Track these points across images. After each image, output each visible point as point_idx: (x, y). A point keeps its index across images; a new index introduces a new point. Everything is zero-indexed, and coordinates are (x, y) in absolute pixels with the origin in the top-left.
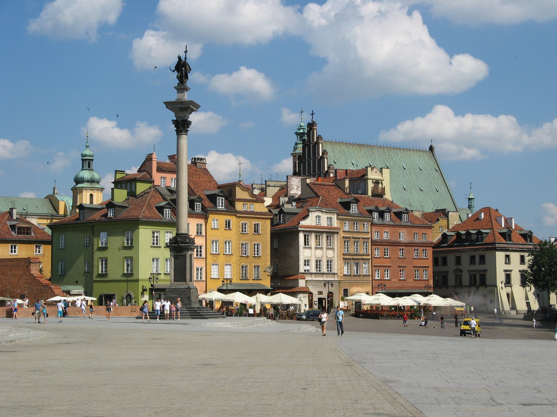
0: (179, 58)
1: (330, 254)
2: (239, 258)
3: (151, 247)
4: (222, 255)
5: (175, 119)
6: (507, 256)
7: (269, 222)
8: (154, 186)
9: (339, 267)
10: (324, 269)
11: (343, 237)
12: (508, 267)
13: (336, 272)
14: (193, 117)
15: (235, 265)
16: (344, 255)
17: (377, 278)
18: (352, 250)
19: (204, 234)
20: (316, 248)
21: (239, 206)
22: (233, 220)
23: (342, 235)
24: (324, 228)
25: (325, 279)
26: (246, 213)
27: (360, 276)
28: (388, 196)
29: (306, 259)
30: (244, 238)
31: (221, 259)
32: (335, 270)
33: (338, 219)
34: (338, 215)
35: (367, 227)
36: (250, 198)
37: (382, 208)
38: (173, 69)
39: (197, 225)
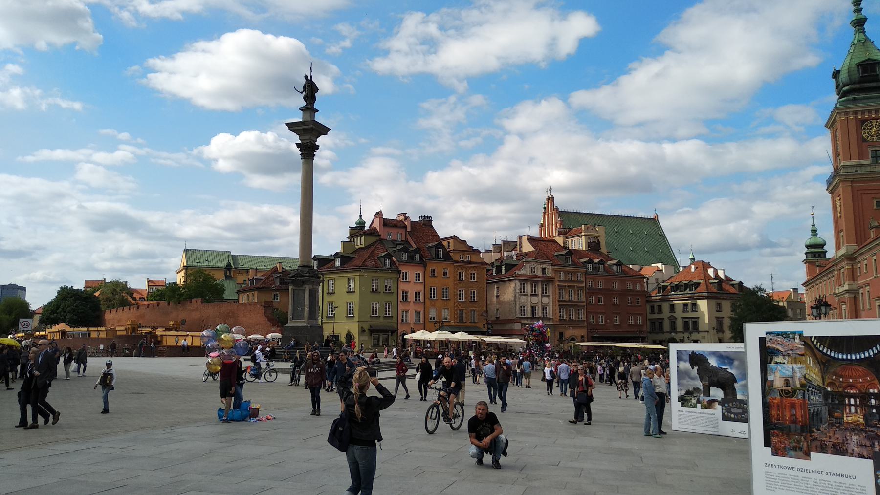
0: (306, 77)
1: (545, 300)
5: (300, 142)
6: (719, 305)
7: (485, 271)
8: (381, 240)
10: (539, 314)
12: (719, 314)
14: (321, 141)
16: (559, 301)
18: (566, 297)
20: (532, 295)
21: (456, 257)
22: (449, 268)
23: (557, 284)
24: (539, 277)
26: (463, 262)
28: (604, 250)
32: (550, 314)
34: (552, 265)
35: (581, 278)
37: (596, 261)
38: (302, 90)
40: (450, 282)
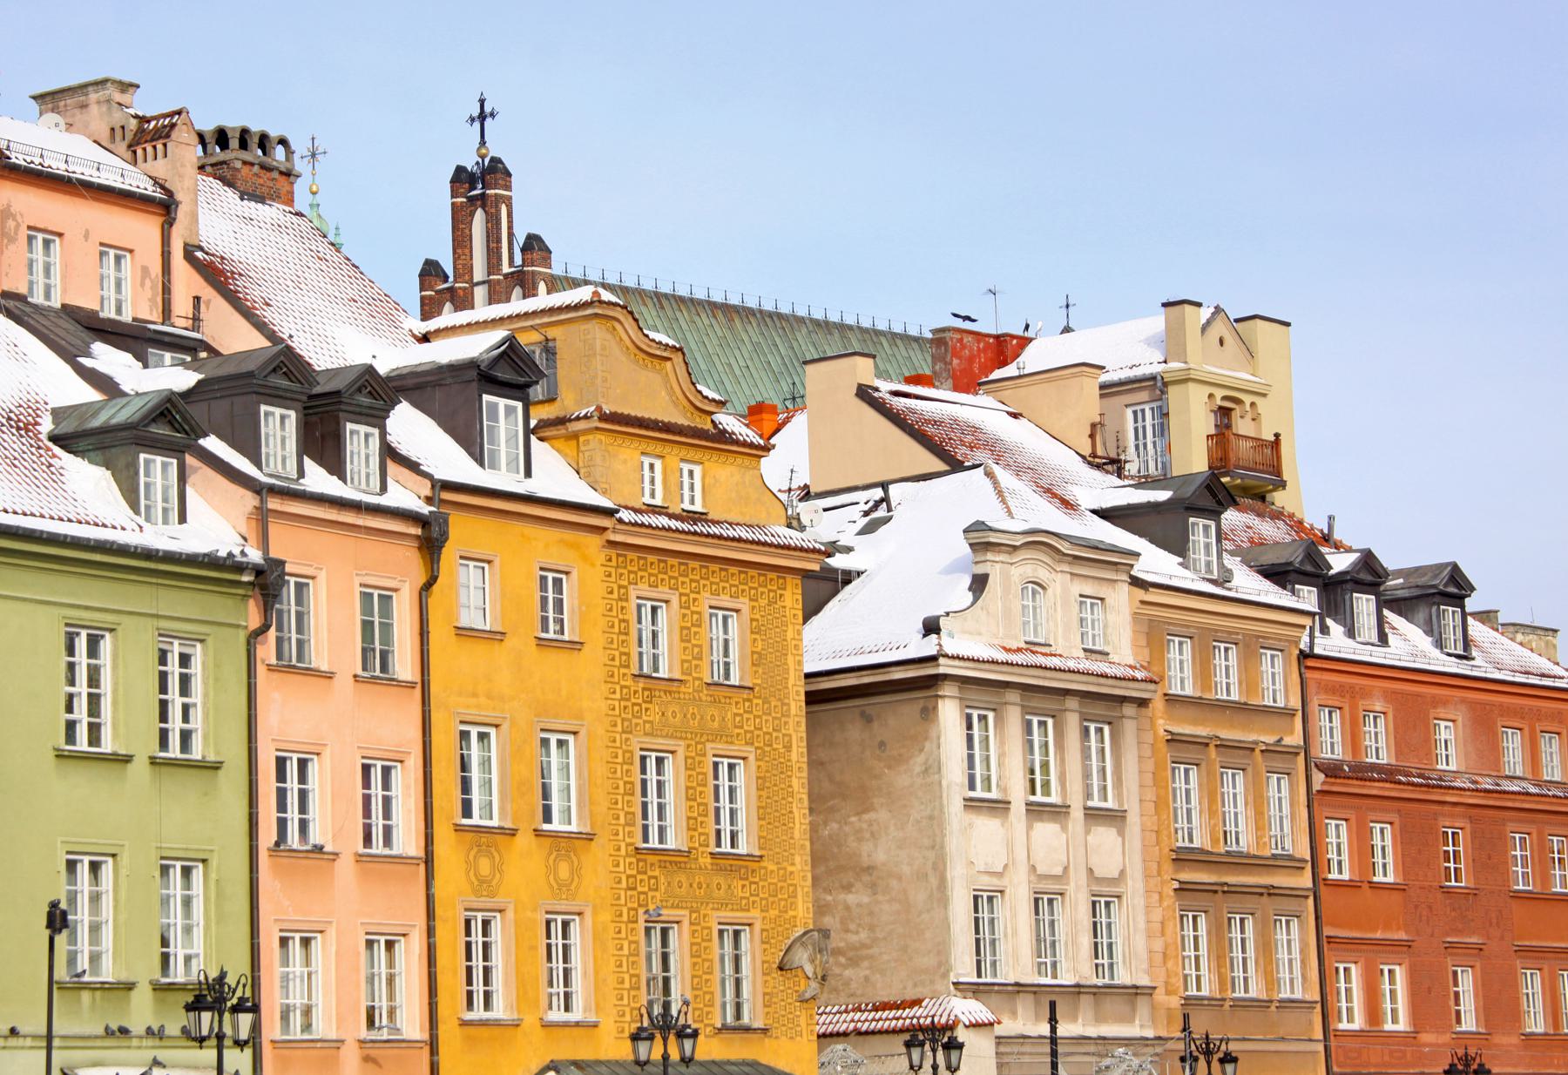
1: (1109, 851)
2: (627, 865)
3: (61, 756)
4: (524, 840)
9: (1158, 945)
11: (1174, 740)
13: (1144, 981)
15: (606, 916)
16: (1183, 858)
17: (1344, 1025)
19: (405, 666)
20: (1036, 811)
23: (1163, 722)
25: (1092, 1031)
27: (1261, 1005)
29: (986, 882)
30: (654, 714)
31: (524, 865)
33: (1136, 616)
35: (1276, 682)
36: (682, 420)
39: (366, 598)
40: (584, 682)
